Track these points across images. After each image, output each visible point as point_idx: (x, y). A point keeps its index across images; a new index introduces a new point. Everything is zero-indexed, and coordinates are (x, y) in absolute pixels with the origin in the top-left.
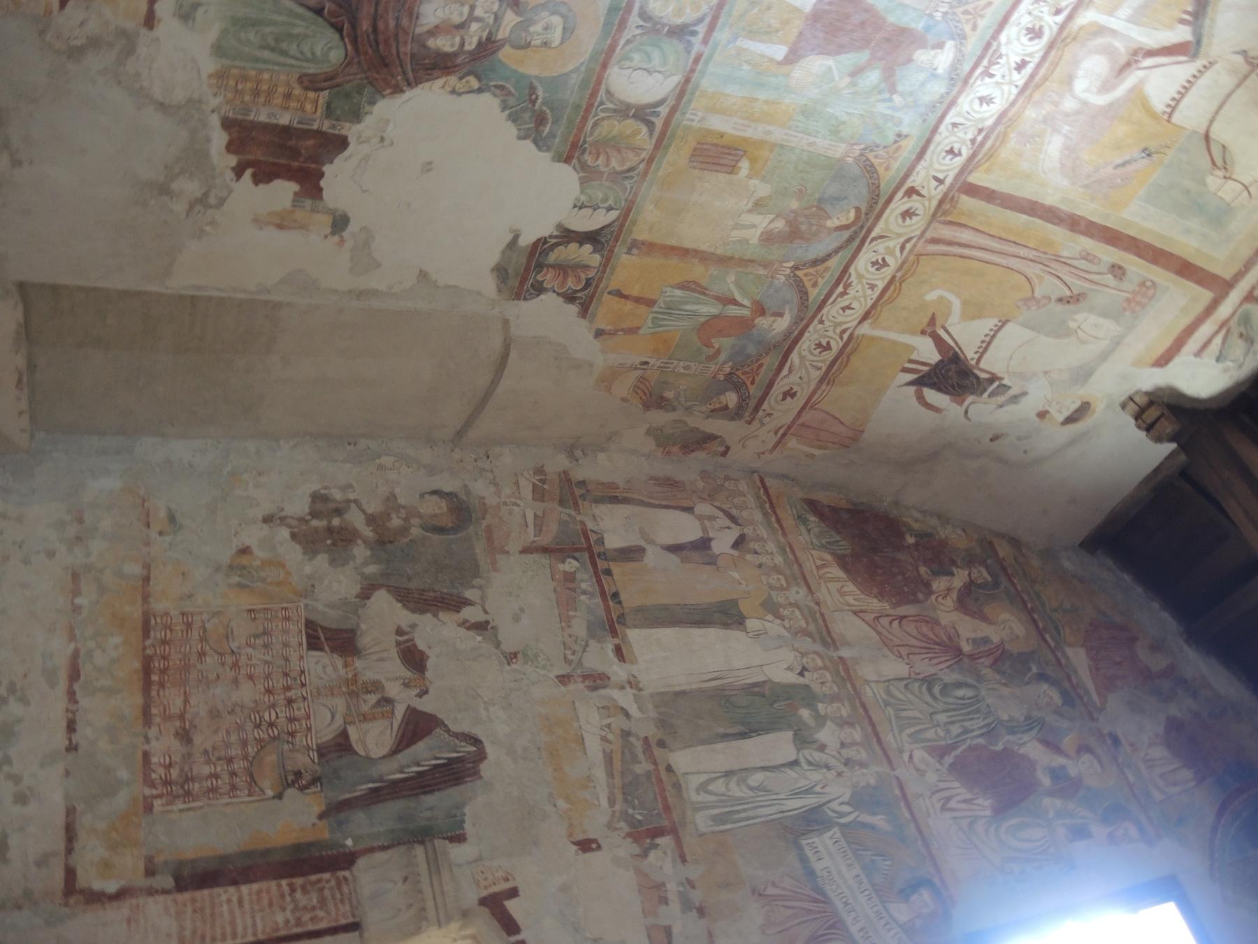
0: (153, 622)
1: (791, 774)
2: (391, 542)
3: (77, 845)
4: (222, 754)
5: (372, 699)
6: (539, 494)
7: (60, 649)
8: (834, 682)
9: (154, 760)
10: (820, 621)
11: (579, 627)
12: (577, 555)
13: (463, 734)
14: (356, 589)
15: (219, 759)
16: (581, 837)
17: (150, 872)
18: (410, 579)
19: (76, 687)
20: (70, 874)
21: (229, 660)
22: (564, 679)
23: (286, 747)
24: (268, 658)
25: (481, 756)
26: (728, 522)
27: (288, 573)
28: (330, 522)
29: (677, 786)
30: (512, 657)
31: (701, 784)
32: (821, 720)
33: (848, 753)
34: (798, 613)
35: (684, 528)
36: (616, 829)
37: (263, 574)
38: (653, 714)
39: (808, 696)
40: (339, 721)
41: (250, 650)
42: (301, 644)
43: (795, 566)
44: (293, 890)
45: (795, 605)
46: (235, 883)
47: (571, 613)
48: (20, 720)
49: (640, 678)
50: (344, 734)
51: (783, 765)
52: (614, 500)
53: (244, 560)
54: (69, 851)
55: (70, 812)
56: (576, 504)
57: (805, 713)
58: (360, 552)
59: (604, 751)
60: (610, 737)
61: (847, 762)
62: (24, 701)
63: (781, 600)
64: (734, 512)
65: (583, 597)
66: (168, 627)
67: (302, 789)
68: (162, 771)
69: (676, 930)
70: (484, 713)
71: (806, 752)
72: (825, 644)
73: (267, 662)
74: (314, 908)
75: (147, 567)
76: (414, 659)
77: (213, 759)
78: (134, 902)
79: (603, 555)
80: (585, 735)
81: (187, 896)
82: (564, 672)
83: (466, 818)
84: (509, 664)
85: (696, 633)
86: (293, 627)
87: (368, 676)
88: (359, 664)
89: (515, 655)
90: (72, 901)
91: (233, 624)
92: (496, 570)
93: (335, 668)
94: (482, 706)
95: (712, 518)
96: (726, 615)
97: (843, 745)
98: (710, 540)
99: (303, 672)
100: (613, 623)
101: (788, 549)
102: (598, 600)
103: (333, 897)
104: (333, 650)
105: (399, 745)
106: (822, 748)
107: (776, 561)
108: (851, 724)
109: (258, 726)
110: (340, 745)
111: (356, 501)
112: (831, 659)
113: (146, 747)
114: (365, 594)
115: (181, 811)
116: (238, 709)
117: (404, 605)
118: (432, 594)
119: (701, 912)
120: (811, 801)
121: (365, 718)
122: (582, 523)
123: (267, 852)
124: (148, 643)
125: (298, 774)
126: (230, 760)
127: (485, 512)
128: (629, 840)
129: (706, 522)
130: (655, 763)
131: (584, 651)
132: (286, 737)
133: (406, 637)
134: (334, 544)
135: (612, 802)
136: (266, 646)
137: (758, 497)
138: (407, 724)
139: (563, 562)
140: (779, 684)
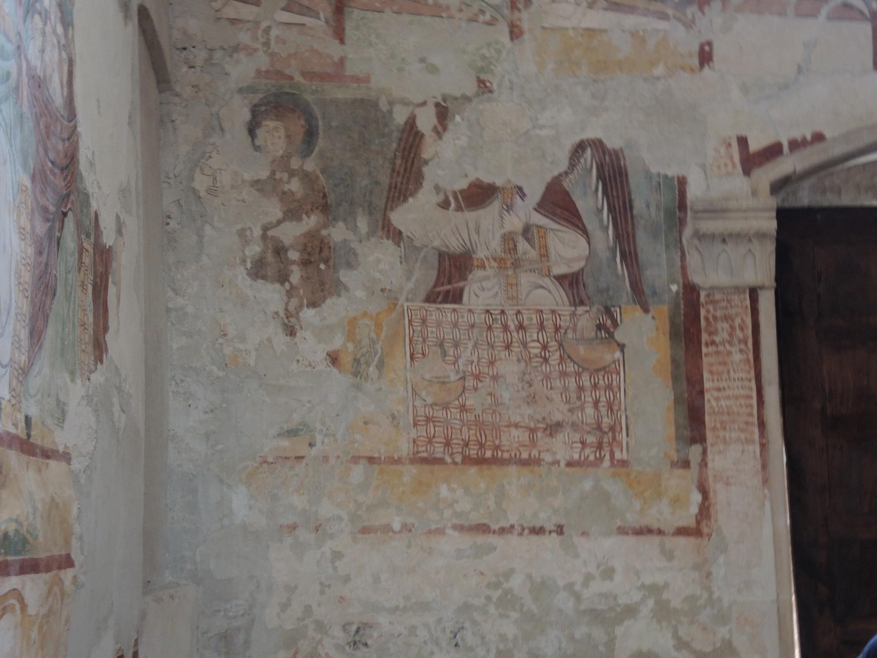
0: (425, 455)
2: (325, 196)
3: (655, 525)
4: (574, 396)
5: (522, 245)
7: (453, 542)
9: (576, 457)
13: (571, 159)
14: (388, 244)
15: (579, 398)
16: (696, 61)
17: (686, 464)
18: (377, 183)
19: (495, 526)
20: (681, 531)
21: (470, 383)
22: (515, 32)
23: (570, 335)
24: (470, 345)
25: (598, 145)
27: (365, 314)
28: (293, 262)
30: (483, 86)
36: (693, 21)
37: (365, 342)
40: (547, 282)
41: (461, 362)
42: (454, 310)
44: (713, 343)
46: (702, 393)
48: (529, 577)
50: (560, 279)
53: (346, 360)
54: (660, 532)
55: (622, 531)
58: (337, 233)
59: (605, 9)
62: (508, 574)
68: (587, 451)
70: (544, 132)
73: (475, 346)
74: (732, 328)
75: (356, 459)
76: (478, 195)
77: (579, 403)
78: (711, 480)
80: (584, 25)
81: (709, 435)
82: (506, 30)
83: (662, 172)
84: (491, 92)
86: (433, 317)
87: (496, 245)
88: (481, 254)
89: (481, 82)
90: (706, 530)
91: (427, 377)
92: (367, 80)
93: (487, 278)
94: (538, 131)
99: (488, 311)
103: (726, 308)
104: (464, 278)
105: (577, 226)
109: (546, 360)
110: (571, 285)
111: (265, 229)
113: (563, 464)
114: (397, 236)
115: (627, 435)
116: (527, 377)
117: (411, 195)
118: (398, 162)
121: (544, 255)
123: (674, 361)
124: (448, 459)
125: (600, 327)
126: (581, 389)
127: (280, 74)
128: (706, 9)
132: (559, 336)
133: (452, 199)
134: (326, 262)
135: (664, 17)
136: (456, 345)
138: (554, 214)
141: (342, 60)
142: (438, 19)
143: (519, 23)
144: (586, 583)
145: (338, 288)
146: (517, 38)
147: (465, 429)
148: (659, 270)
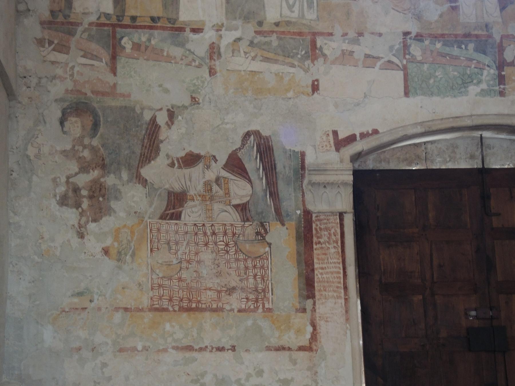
0: (157, 306)
2: (103, 160)
3: (287, 346)
4: (243, 272)
6: (63, 48)
7: (172, 356)
9: (243, 306)
11: (177, 52)
12: (118, 36)
13: (242, 141)
14: (140, 187)
15: (246, 273)
16: (310, 90)
17: (304, 310)
18: (134, 153)
19: (196, 347)
20: (301, 349)
21: (184, 265)
22: (212, 72)
23: (241, 238)
24: (185, 243)
25: (257, 133)
27: (125, 226)
28: (84, 197)
29: (288, 23)
30: (194, 101)
31: (288, 8)
36: (308, 68)
37: (125, 242)
38: (239, 22)
40: (229, 208)
41: (179, 253)
42: (176, 224)
44: (319, 243)
46: (313, 270)
47: (165, 54)
48: (215, 375)
49: (215, 23)
50: (236, 206)
53: (113, 252)
54: (289, 349)
55: (268, 349)
56: (72, 24)
58: (110, 180)
59: (261, 61)
60: (253, 54)
65: (153, 42)
66: (161, 298)
67: (266, 232)
68: (250, 303)
69: (368, 52)
70: (228, 126)
73: (188, 244)
74: (330, 234)
75: (117, 309)
76: (191, 160)
77: (245, 276)
78: (318, 319)
79: (120, 17)
80: (249, 69)
81: (317, 294)
82: (207, 71)
83: (292, 149)
84: (199, 104)
86: (164, 228)
87: (200, 187)
88: (192, 192)
89: (193, 98)
90: (315, 348)
91: (160, 262)
92: (129, 96)
93: (195, 206)
94: (224, 126)
99: (195, 224)
102: (156, 32)
103: (326, 223)
104: (182, 206)
105: (246, 178)
109: (227, 252)
110: (242, 210)
111: (68, 178)
113: (236, 311)
114: (144, 182)
115: (272, 294)
116: (217, 262)
117: (153, 159)
118: (146, 141)
119: (361, 34)
122: (91, 24)
123: (299, 253)
124: (171, 309)
125: (258, 233)
126: (247, 268)
127: (79, 92)
128: (315, 62)
130: (273, 32)
131: (193, 53)
132: (234, 239)
133: (176, 162)
134: (103, 196)
135: (293, 66)
136: (177, 243)
138: (233, 171)
139: (124, 48)
141: (115, 85)
142: (169, 64)
143: (214, 67)
144: (247, 380)
145: (109, 211)
146: (213, 75)
147: (181, 291)
148: (290, 202)
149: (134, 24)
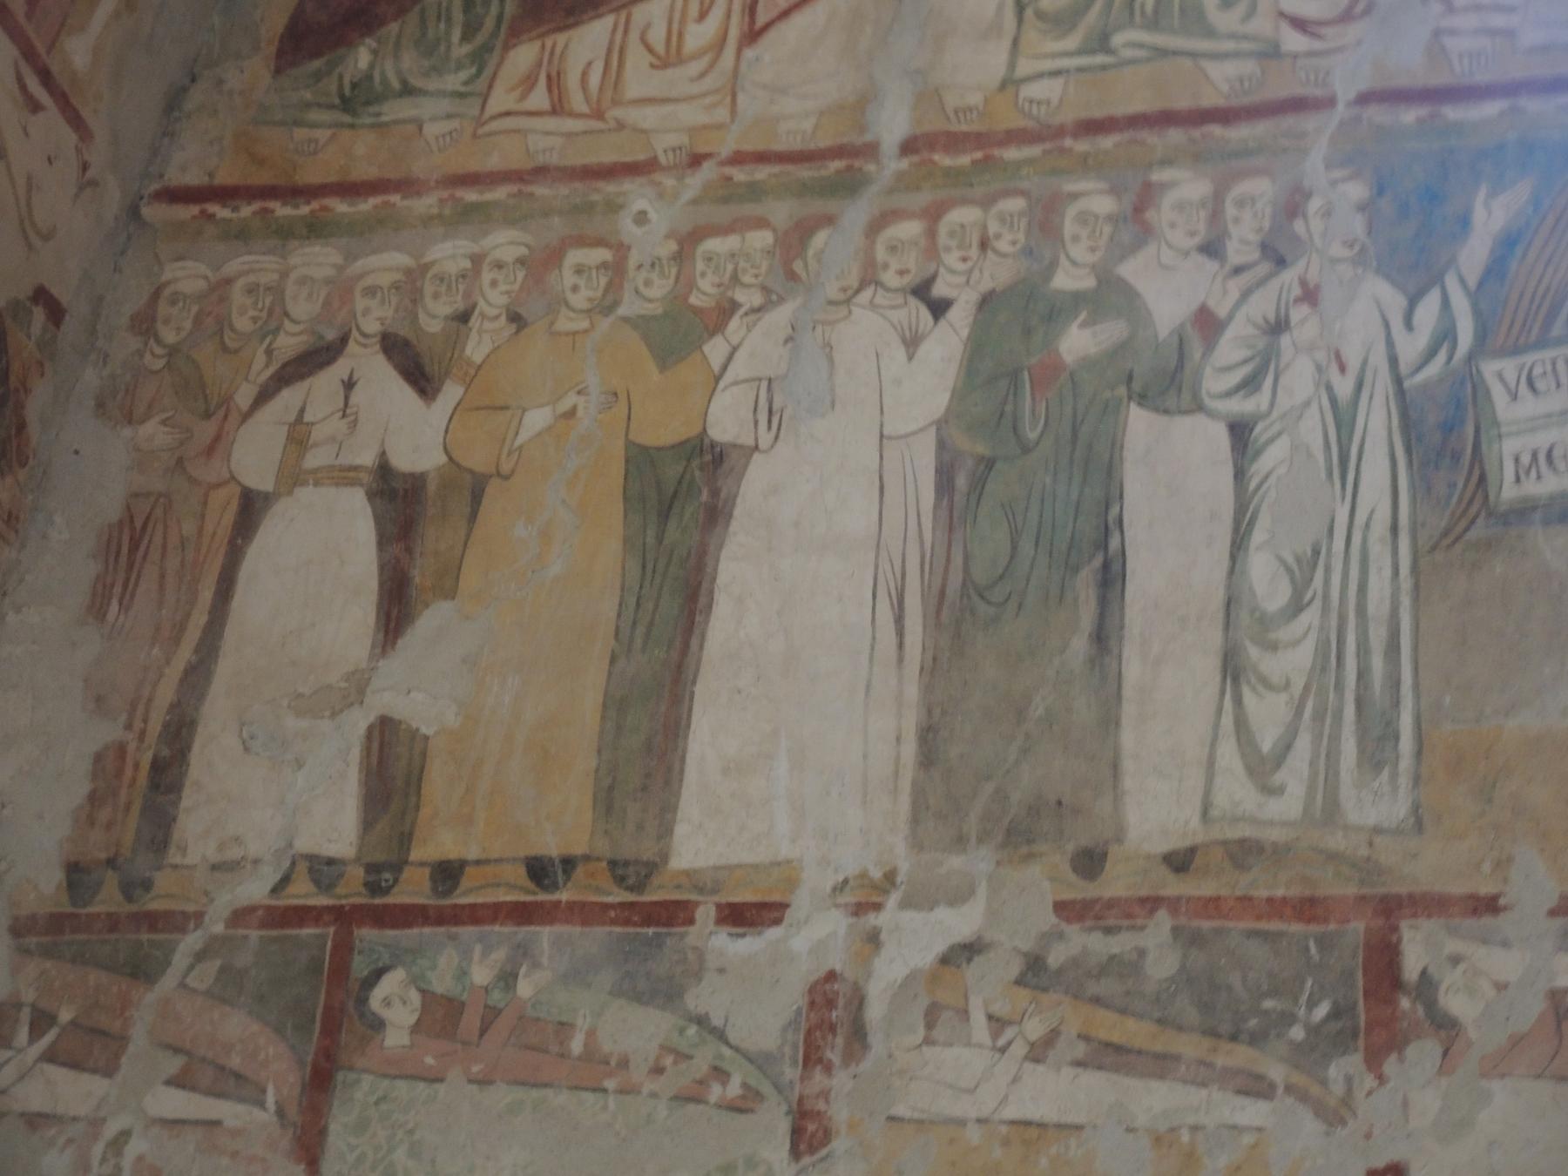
1: (1272, 458)
6: (92, 1047)
8: (987, 203)
10: (762, 173)
11: (636, 1031)
12: (360, 967)
22: (808, 1133)
26: (326, 382)
29: (1243, 853)
31: (1251, 771)
32: (1110, 297)
33: (1242, 241)
34: (713, 245)
35: (317, 554)
36: (1347, 1101)
38: (980, 861)
39: (1016, 321)
43: (541, 190)
45: (688, 241)
47: (577, 1045)
49: (851, 869)
51: (1240, 475)
52: (167, 774)
56: (153, 921)
57: (1078, 342)
59: (1079, 1064)
60: (1035, 1028)
61: (1275, 256)
63: (660, 288)
64: (289, 343)
65: (525, 988)
71: (1214, 383)
72: (849, 185)
79: (380, 874)
80: (1010, 1113)
82: (784, 1126)
85: (725, 627)
95: (298, 436)
96: (680, 497)
97: (1212, 249)
98: (384, 469)
100: (649, 915)
101: (470, 193)
102: (545, 935)
106: (1208, 324)
107: (509, 254)
108: (1146, 197)
112: (903, 183)
120: (1377, 421)
122: (239, 917)
128: (1390, 1066)
129: (314, 460)
130: (1152, 903)
131: (720, 1035)
135: (1256, 1087)
137: (240, 235)
139: (379, 1025)
140: (958, 396)
142: (589, 1097)
143: (821, 1106)
146: (812, 1150)
149: (449, 902)
